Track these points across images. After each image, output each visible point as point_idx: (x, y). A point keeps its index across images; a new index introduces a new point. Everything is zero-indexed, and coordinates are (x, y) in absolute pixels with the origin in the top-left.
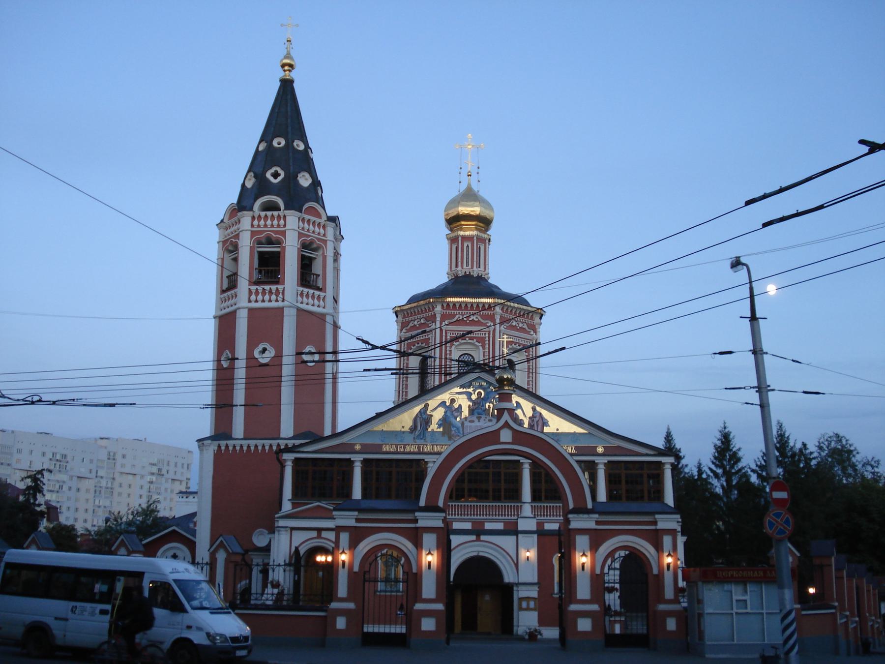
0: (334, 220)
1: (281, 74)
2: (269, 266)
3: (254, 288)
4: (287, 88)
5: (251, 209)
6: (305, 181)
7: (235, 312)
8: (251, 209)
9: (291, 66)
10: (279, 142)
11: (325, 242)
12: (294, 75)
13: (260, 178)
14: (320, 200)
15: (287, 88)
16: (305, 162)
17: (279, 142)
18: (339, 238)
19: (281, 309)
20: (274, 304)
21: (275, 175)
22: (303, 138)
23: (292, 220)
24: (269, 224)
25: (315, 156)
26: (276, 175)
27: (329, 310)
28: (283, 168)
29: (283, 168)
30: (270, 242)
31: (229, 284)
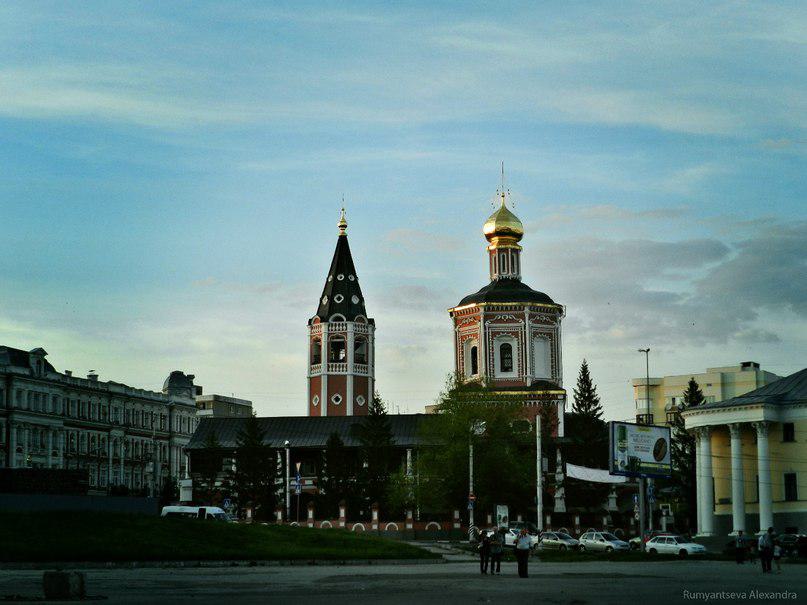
0: (371, 321)
1: (339, 232)
2: (337, 346)
3: (330, 364)
4: (343, 243)
5: (327, 321)
6: (355, 300)
7: (320, 376)
8: (327, 321)
9: (346, 226)
10: (341, 277)
11: (367, 336)
12: (346, 231)
13: (331, 299)
14: (363, 311)
15: (343, 243)
16: (354, 288)
17: (341, 277)
18: (374, 329)
19: (345, 376)
20: (341, 373)
21: (339, 299)
22: (353, 273)
23: (350, 326)
24: (338, 329)
25: (361, 282)
26: (339, 299)
27: (370, 375)
28: (343, 294)
29: (343, 294)
30: (338, 337)
31: (315, 359)
